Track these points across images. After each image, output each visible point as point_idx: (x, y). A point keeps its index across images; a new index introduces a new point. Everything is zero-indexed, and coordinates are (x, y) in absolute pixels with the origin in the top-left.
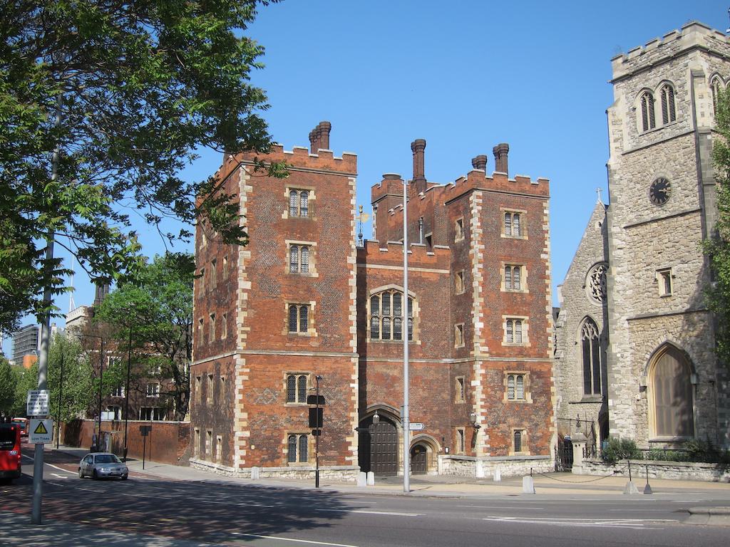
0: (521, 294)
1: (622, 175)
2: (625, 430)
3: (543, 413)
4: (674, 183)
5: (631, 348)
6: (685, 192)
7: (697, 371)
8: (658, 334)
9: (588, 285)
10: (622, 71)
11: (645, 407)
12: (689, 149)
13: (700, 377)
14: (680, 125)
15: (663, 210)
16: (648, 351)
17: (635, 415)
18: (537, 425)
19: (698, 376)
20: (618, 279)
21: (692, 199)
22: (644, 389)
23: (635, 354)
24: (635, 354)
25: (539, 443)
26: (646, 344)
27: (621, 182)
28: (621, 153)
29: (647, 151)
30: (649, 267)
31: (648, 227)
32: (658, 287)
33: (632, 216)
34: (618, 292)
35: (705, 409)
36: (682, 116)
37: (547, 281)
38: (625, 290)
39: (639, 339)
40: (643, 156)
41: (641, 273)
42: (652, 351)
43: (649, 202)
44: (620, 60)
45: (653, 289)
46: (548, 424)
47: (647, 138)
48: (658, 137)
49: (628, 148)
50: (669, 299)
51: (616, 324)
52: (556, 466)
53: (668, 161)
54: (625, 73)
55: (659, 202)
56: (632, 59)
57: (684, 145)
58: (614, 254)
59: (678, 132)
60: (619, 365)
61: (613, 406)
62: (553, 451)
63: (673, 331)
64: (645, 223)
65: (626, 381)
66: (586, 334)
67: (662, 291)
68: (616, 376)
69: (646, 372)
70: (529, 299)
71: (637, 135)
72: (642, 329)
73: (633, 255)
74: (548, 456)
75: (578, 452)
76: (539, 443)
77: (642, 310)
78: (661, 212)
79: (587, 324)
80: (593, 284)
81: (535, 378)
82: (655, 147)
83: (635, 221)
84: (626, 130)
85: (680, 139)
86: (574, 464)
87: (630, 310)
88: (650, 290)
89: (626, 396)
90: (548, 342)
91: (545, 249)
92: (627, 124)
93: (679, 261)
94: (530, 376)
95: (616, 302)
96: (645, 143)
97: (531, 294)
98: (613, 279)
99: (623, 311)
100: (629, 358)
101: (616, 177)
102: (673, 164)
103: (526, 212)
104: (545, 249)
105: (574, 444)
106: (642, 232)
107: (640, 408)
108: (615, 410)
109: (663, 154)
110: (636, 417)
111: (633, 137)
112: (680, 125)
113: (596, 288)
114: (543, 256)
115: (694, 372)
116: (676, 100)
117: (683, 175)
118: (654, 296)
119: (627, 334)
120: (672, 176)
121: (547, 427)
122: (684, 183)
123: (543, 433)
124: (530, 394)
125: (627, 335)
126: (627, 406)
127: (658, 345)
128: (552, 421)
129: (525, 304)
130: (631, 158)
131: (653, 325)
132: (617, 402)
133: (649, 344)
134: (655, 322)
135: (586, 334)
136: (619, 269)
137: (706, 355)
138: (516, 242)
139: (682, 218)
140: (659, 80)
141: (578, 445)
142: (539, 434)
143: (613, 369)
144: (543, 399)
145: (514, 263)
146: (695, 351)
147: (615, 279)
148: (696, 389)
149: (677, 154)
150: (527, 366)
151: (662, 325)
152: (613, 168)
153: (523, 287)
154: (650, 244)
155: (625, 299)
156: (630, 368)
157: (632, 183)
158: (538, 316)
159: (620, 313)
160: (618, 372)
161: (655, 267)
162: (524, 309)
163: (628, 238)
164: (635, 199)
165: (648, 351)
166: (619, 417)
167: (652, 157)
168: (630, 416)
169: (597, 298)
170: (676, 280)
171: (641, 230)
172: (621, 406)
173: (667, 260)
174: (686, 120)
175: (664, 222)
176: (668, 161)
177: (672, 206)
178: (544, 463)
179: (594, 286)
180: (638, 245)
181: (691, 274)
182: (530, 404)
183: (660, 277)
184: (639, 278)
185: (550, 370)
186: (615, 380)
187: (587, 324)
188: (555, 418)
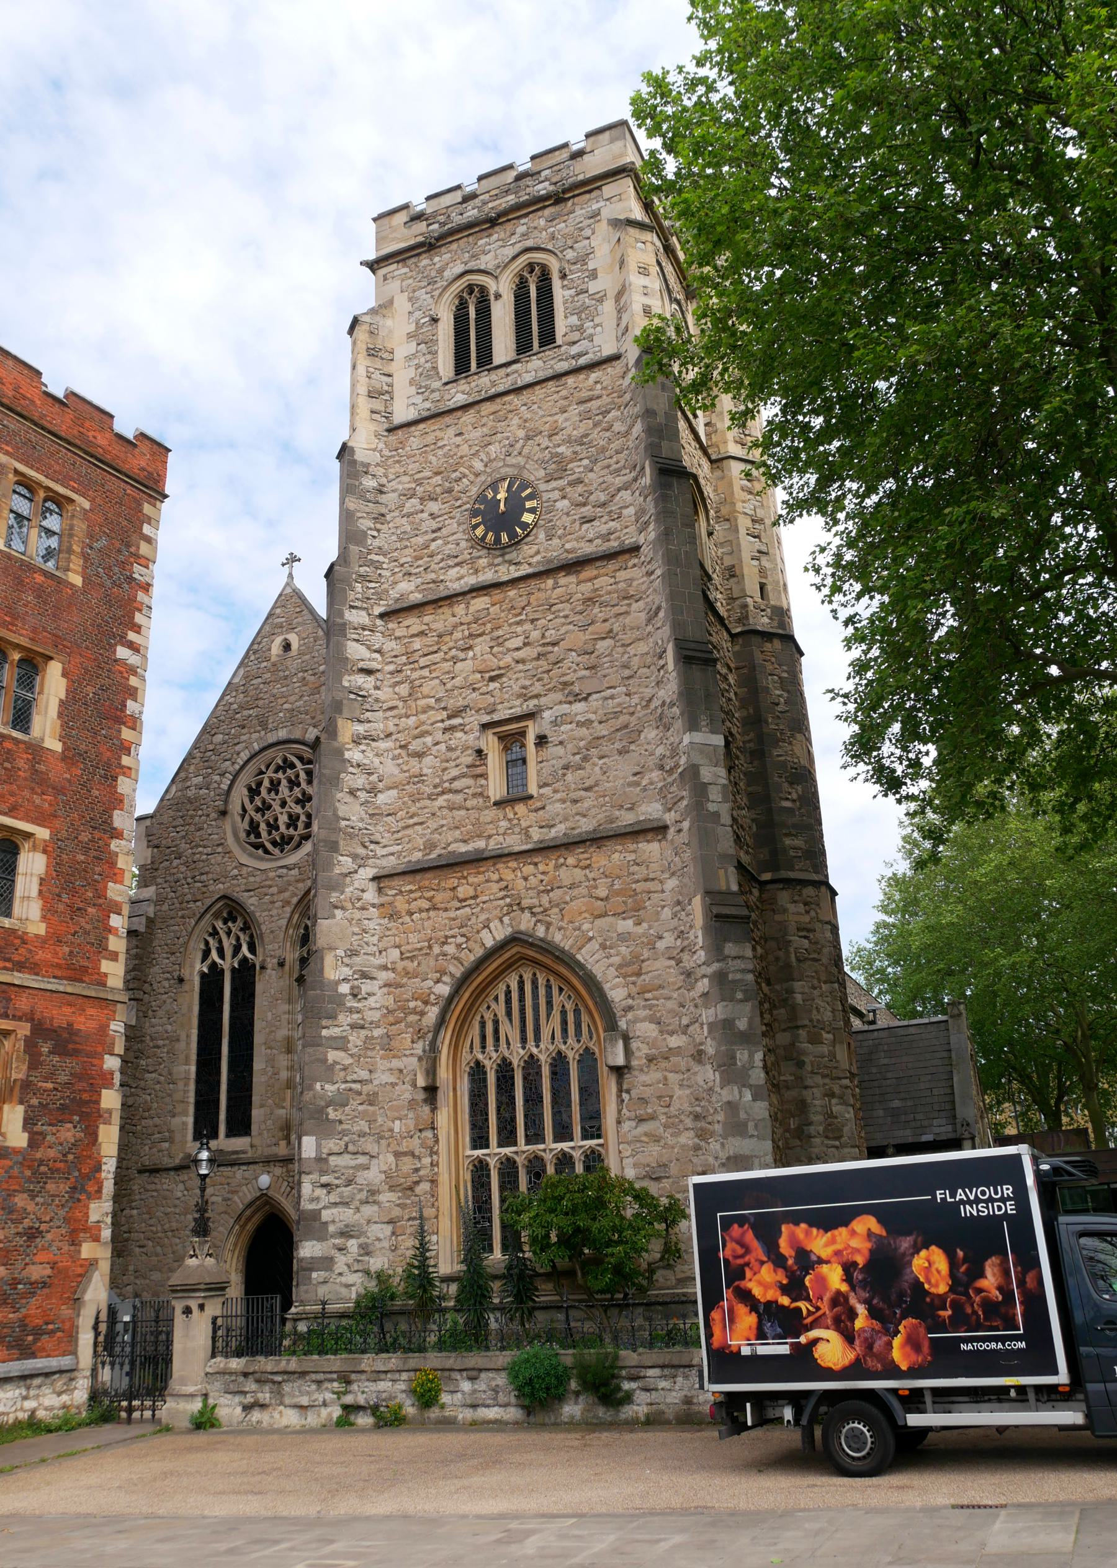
0: (36, 750)
1: (384, 481)
2: (353, 1245)
3: (64, 1187)
4: (549, 491)
5: (385, 968)
6: (583, 509)
7: (623, 1024)
8: (483, 917)
9: (235, 807)
10: (406, 240)
11: (427, 1161)
12: (594, 404)
13: (634, 1045)
14: (574, 350)
15: (511, 563)
16: (443, 972)
17: (392, 1188)
18: (32, 1234)
19: (626, 1039)
20: (354, 754)
21: (604, 529)
22: (431, 1090)
23: (399, 986)
24: (399, 986)
25: (32, 1308)
26: (436, 950)
27: (383, 498)
28: (386, 426)
29: (468, 417)
30: (456, 721)
31: (460, 609)
32: (484, 776)
33: (404, 586)
34: (352, 793)
35: (655, 1149)
36: (580, 329)
37: (126, 734)
38: (373, 791)
39: (413, 938)
40: (451, 432)
41: (429, 740)
42: (458, 971)
43: (463, 544)
44: (402, 217)
45: (469, 781)
46: (78, 1230)
47: (466, 388)
48: (498, 381)
49: (402, 412)
50: (521, 808)
51: (337, 886)
52: (95, 1396)
53: (528, 438)
54: (412, 242)
55: (498, 540)
56: (435, 214)
57: (585, 394)
58: (346, 684)
59: (563, 366)
60: (344, 1019)
61: (320, 1160)
62: (86, 1339)
63: (535, 901)
64: (450, 599)
65: (364, 1074)
66: (214, 955)
67: (496, 788)
68: (332, 1055)
69: (434, 1048)
70: (58, 773)
71: (437, 384)
72: (426, 905)
73: (403, 689)
74: (66, 1362)
75: (191, 1338)
76: (32, 1308)
77: (430, 846)
78: (503, 569)
79: (219, 925)
80: (249, 806)
81: (45, 1050)
82: (488, 408)
83: (417, 597)
84: (402, 376)
85: (570, 380)
86: (174, 1385)
87: (385, 851)
88: (457, 785)
89: (363, 1125)
90: (110, 930)
91: (132, 636)
92: (408, 358)
93: (559, 696)
94: (30, 1045)
95: (343, 823)
96: (460, 399)
97: (70, 756)
98: (339, 752)
99: (361, 851)
100: (377, 999)
101: (369, 483)
102: (545, 442)
103: (87, 505)
104: (132, 636)
105: (179, 1306)
106: (439, 626)
107: (407, 1164)
108: (323, 1172)
109: (516, 421)
110: (392, 1196)
111: (422, 390)
112: (574, 350)
113: (258, 817)
114: (122, 652)
115: (611, 1025)
116: (560, 294)
117: (577, 468)
118: (469, 804)
119: (375, 922)
120: (542, 473)
121: (75, 1243)
122: (580, 488)
123: (53, 1265)
124: (20, 1110)
125: (371, 925)
126: (362, 1160)
127: (479, 952)
128: (93, 1217)
129: (39, 780)
130: (415, 440)
131: (464, 891)
132: (332, 1145)
133: (450, 949)
134: (471, 879)
135: (214, 955)
136: (361, 728)
137: (659, 968)
138: (39, 578)
139: (572, 579)
140: (510, 252)
141: (194, 1305)
142: (37, 1272)
143: (324, 1032)
144: (68, 1133)
145: (24, 642)
146: (616, 960)
147: (347, 755)
148: (620, 1084)
149: (560, 418)
150: (23, 1003)
151: (495, 887)
152: (360, 456)
153: (46, 727)
154: (462, 655)
155: (372, 815)
156: (377, 1033)
157: (414, 501)
158: (85, 837)
159: (355, 857)
160: (341, 1043)
161: (473, 720)
162: (37, 800)
163: (390, 645)
164: (420, 540)
165: (443, 972)
166: (333, 1198)
167: (478, 433)
168: (373, 1192)
169: (257, 846)
170: (552, 750)
171: (439, 620)
172: (345, 1161)
173: (519, 696)
174: (591, 339)
175: (512, 593)
176: (528, 438)
177: (537, 551)
178: (46, 1390)
179: (253, 813)
180: (423, 662)
181: (603, 730)
182: (16, 1151)
183: (491, 744)
184: (420, 755)
185: (104, 1028)
186: (329, 1071)
187: (219, 925)
188: (107, 1206)
